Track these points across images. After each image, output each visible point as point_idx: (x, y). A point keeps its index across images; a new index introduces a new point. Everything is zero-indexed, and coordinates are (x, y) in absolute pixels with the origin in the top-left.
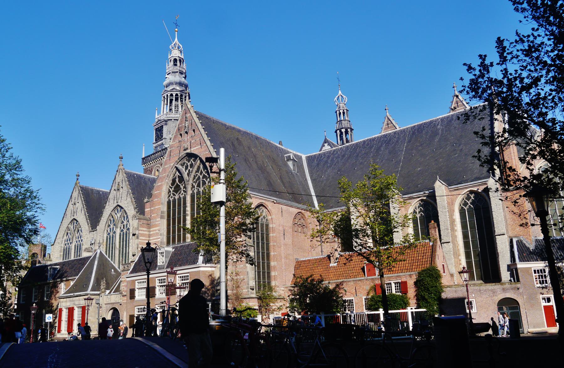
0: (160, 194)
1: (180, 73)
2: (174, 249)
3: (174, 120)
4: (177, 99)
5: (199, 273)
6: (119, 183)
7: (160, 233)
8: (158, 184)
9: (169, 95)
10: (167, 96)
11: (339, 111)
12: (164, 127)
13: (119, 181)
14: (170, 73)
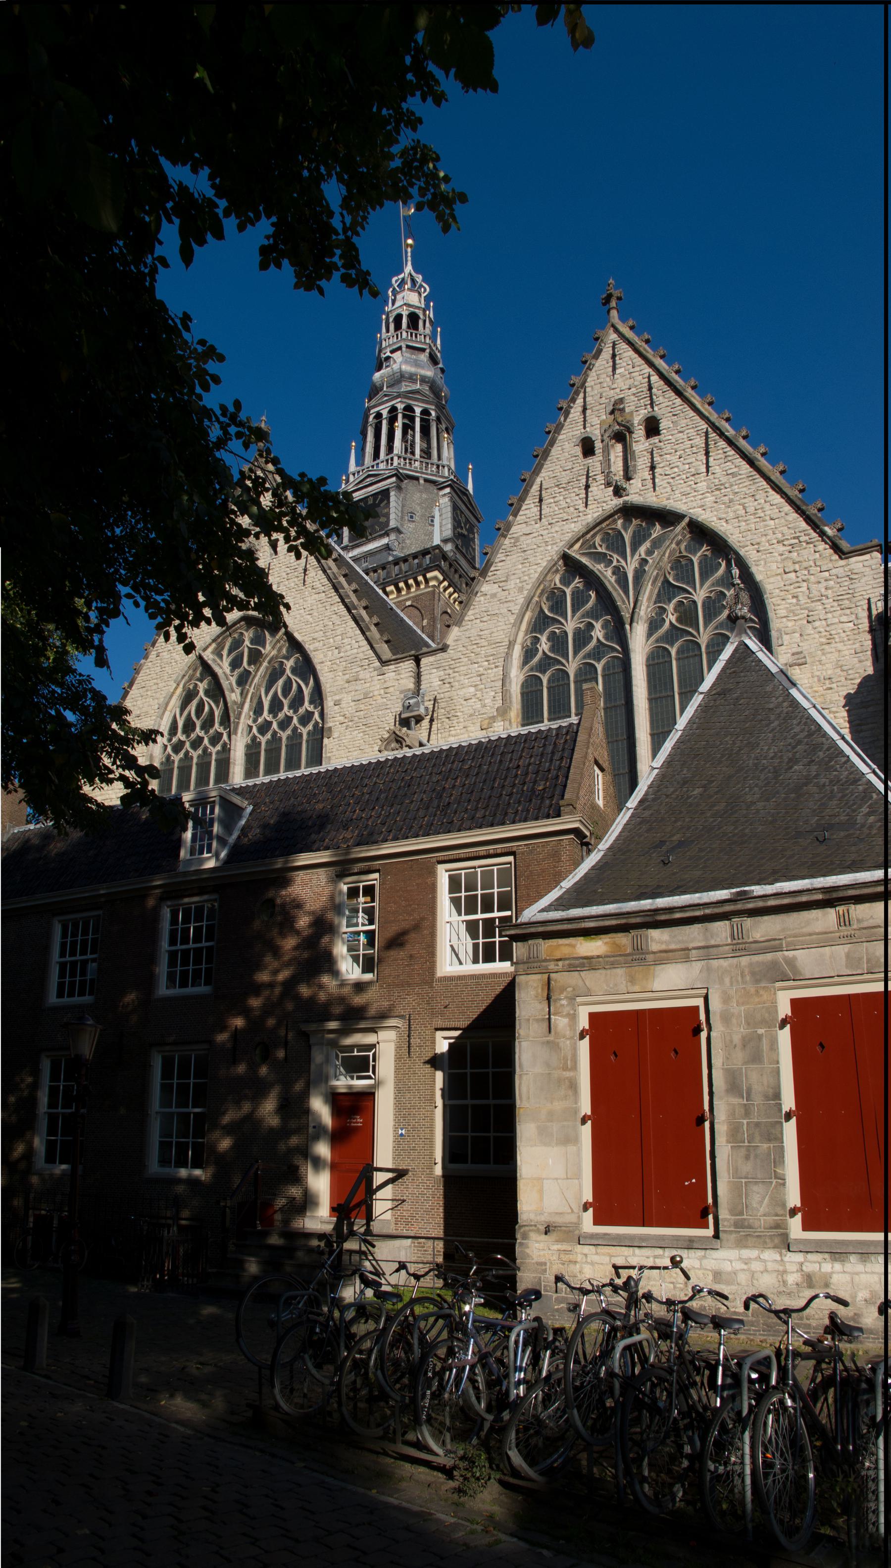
1: (430, 354)
3: (426, 480)
9: (400, 407)
10: (393, 409)
12: (392, 493)
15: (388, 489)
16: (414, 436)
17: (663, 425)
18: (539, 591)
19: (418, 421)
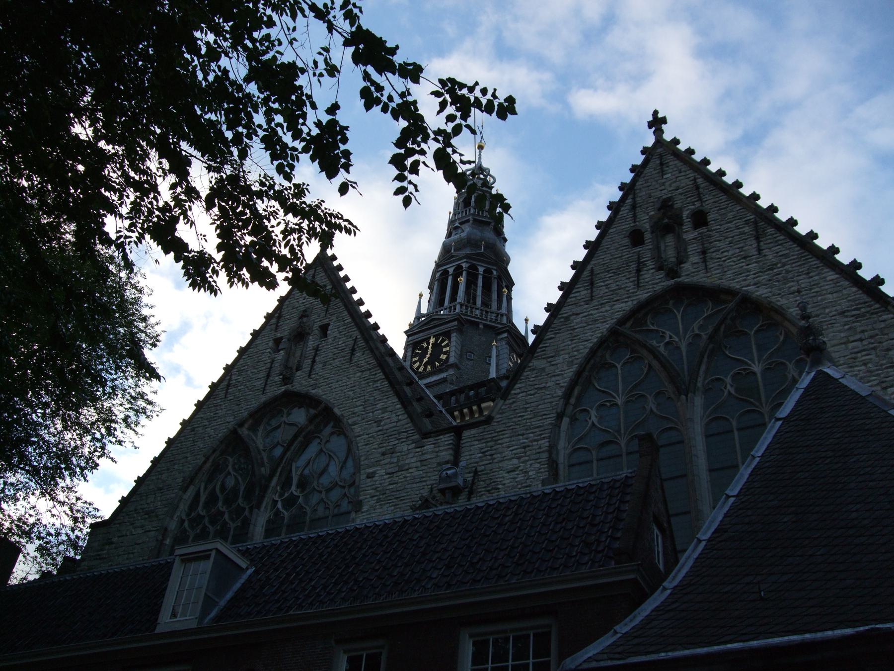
3: (485, 325)
14: (468, 221)
15: (449, 331)
16: (475, 290)
17: (711, 217)
18: (589, 366)
19: (480, 278)
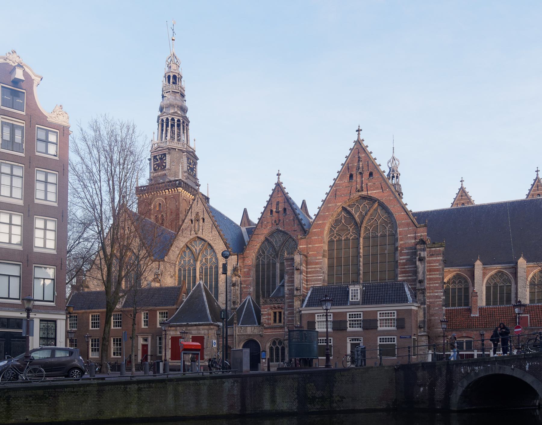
0: (322, 232)
2: (364, 288)
4: (179, 126)
5: (411, 311)
6: (198, 213)
7: (322, 271)
8: (318, 222)
9: (170, 119)
10: (167, 119)
11: (393, 174)
13: (197, 210)
16: (175, 129)
19: (176, 124)
